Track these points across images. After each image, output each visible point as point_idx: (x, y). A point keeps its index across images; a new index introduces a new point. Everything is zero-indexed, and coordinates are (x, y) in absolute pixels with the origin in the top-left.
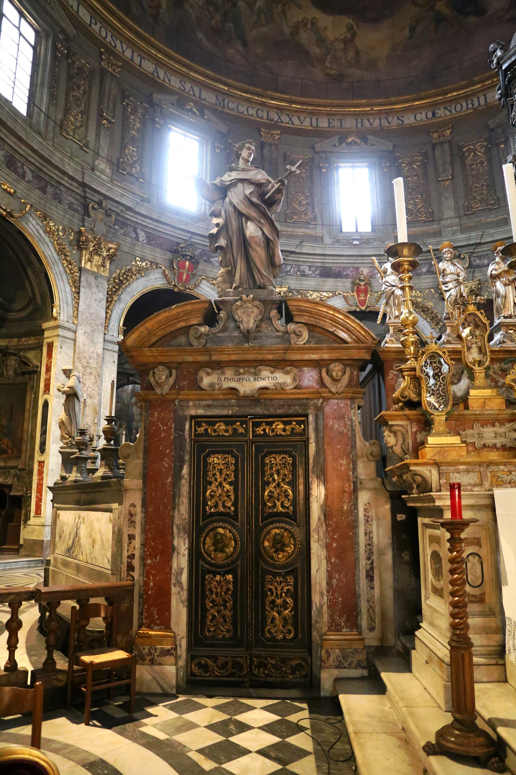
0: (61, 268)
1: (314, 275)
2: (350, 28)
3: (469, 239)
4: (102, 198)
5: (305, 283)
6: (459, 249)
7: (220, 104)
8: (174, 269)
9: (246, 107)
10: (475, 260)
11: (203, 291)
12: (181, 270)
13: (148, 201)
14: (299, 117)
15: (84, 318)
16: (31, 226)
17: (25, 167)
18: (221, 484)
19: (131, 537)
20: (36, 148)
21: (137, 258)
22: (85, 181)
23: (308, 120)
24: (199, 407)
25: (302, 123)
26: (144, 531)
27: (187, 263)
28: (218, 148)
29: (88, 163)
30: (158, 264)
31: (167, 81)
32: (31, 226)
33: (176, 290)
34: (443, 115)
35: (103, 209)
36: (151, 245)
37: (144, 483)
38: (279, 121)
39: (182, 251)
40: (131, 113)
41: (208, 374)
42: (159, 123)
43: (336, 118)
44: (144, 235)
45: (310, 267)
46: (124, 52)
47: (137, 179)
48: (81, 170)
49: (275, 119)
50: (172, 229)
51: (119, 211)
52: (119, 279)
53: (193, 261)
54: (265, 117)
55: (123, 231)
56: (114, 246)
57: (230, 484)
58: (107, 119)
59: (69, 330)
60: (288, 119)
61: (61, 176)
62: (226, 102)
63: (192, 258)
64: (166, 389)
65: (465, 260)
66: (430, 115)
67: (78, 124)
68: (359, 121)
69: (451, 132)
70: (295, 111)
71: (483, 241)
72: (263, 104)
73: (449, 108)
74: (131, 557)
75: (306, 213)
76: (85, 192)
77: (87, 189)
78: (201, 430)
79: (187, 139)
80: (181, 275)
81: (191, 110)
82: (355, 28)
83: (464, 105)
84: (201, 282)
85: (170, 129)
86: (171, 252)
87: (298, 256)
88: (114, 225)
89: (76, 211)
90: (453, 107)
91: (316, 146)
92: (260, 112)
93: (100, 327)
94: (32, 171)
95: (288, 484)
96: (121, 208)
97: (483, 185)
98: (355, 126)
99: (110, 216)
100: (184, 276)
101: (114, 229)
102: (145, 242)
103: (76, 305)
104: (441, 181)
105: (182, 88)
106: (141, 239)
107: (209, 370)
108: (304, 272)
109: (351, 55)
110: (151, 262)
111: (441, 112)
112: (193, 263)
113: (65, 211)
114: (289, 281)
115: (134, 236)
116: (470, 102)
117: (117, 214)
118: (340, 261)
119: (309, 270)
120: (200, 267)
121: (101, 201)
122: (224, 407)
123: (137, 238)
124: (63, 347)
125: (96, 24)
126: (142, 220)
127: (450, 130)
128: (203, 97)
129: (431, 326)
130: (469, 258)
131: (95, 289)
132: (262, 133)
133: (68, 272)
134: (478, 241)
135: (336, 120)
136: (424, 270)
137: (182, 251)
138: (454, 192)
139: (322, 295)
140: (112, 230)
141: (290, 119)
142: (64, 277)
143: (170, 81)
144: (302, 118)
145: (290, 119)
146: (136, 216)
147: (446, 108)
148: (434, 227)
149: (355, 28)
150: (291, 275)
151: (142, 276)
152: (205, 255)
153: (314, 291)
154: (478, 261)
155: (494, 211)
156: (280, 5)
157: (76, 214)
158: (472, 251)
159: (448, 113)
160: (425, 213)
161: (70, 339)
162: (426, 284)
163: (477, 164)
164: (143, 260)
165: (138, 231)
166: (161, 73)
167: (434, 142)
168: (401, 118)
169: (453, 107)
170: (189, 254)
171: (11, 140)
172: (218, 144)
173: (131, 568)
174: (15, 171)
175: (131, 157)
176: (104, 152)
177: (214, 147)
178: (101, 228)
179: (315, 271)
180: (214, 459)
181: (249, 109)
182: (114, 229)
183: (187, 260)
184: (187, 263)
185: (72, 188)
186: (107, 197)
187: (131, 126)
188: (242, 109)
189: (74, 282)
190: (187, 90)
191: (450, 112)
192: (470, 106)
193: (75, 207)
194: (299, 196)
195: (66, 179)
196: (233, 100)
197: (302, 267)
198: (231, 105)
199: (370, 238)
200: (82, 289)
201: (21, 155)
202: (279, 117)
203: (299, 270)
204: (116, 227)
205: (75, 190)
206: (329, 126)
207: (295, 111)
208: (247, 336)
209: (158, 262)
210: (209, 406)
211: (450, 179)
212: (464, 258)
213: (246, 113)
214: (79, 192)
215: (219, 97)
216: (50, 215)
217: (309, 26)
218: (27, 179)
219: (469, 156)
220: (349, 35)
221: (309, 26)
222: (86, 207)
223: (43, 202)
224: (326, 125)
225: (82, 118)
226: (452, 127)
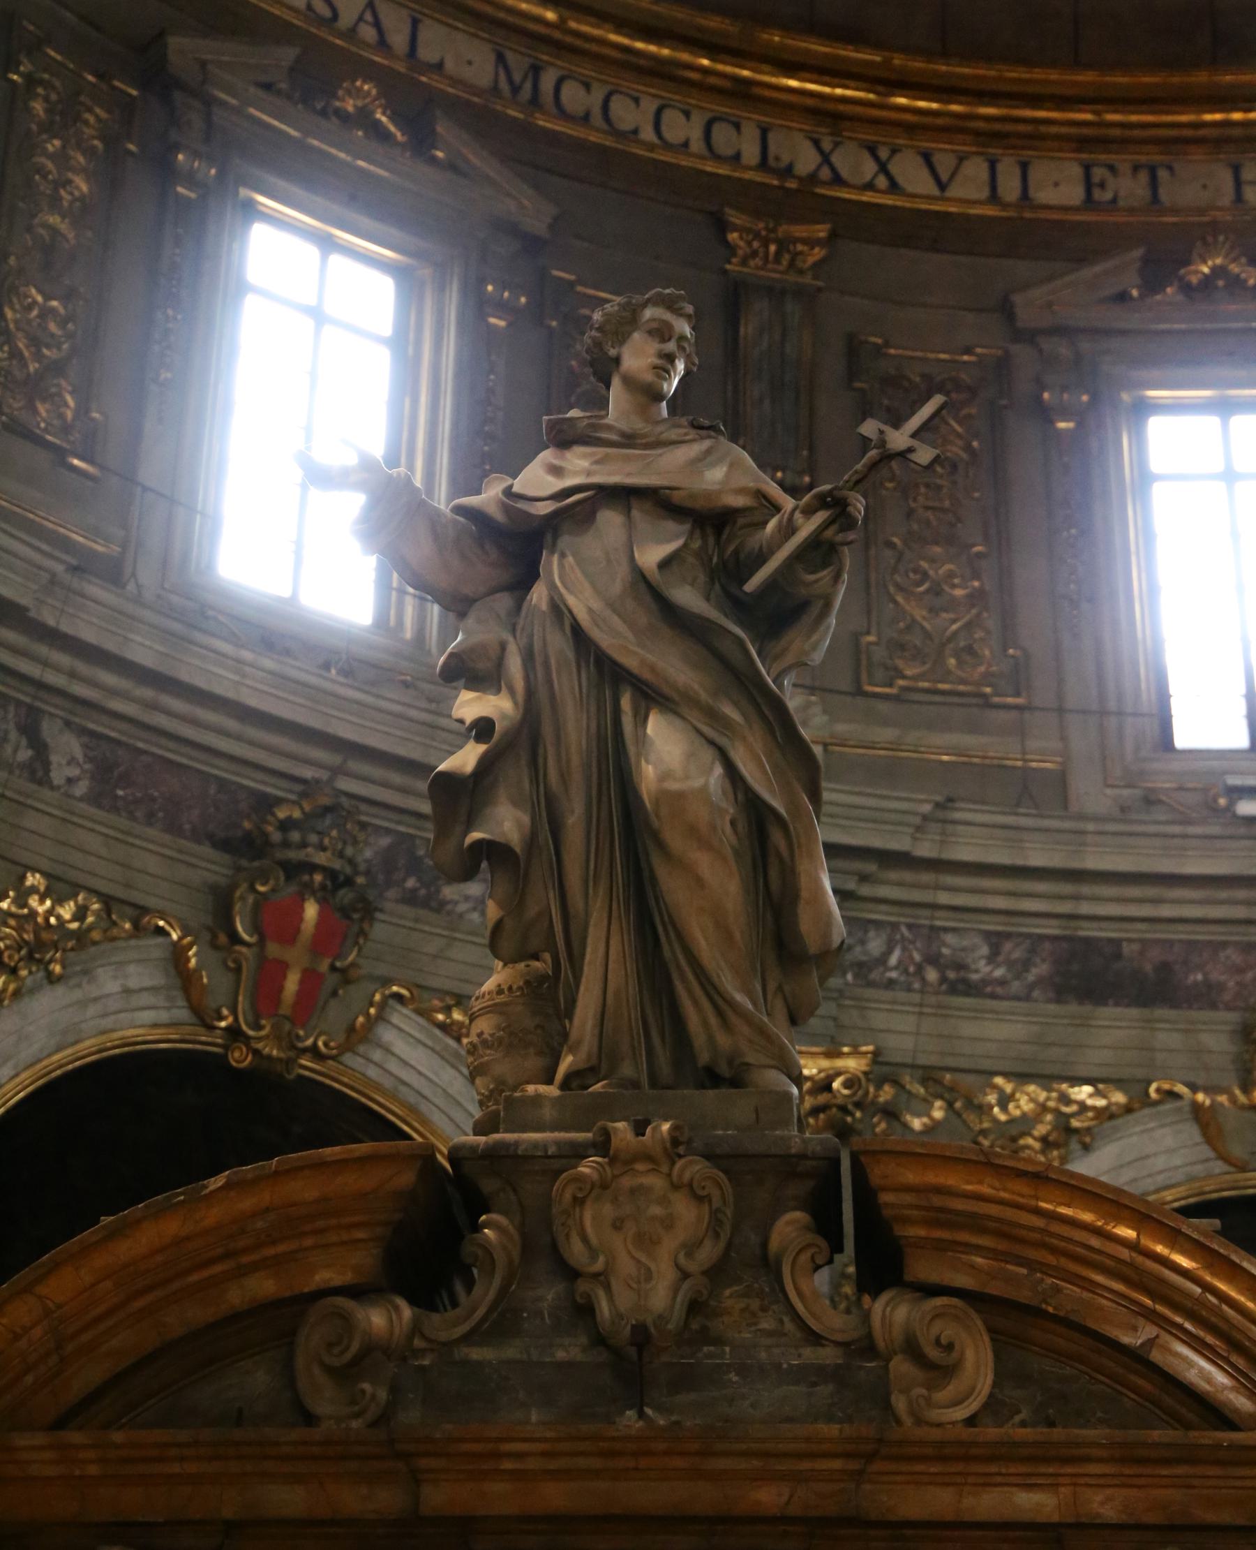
1: (1016, 986)
5: (969, 1029)
7: (516, 90)
8: (235, 938)
9: (649, 106)
11: (393, 1066)
12: (273, 949)
14: (927, 157)
21: (32, 880)
23: (976, 169)
25: (942, 186)
27: (311, 911)
28: (502, 308)
30: (144, 910)
33: (239, 1058)
36: (115, 809)
38: (825, 173)
39: (286, 844)
40: (49, 129)
42: (191, 180)
43: (1123, 161)
44: (78, 753)
45: (996, 940)
47: (60, 454)
50: (232, 724)
53: (345, 896)
54: (751, 153)
60: (869, 168)
62: (548, 81)
63: (337, 881)
70: (910, 129)
72: (742, 92)
75: (970, 650)
79: (336, 259)
80: (271, 973)
81: (363, 119)
84: (380, 1017)
85: (250, 212)
86: (224, 845)
87: (927, 877)
91: (1017, 299)
92: (722, 134)
100: (292, 984)
102: (81, 789)
106: (57, 777)
108: (960, 966)
110: (109, 902)
112: (345, 912)
114: (879, 1020)
115: (25, 754)
118: (1166, 911)
119: (992, 959)
120: (379, 931)
123: (38, 769)
126: (72, 675)
128: (427, 53)
132: (733, 237)
135: (1125, 168)
137: (286, 844)
139: (1065, 1099)
144: (944, 163)
145: (883, 168)
146: (43, 650)
150: (891, 984)
151: (52, 979)
152: (414, 866)
153: (1022, 1078)
164: (59, 889)
165: (49, 730)
170: (321, 858)
175: (35, 342)
179: (1026, 964)
181: (668, 115)
183: (307, 890)
184: (311, 911)
187: (45, 188)
188: (626, 114)
190: (345, 21)
194: (932, 561)
196: (587, 71)
197: (950, 938)
198: (573, 96)
202: (826, 159)
203: (933, 959)
207: (910, 129)
209: (151, 902)
213: (648, 134)
215: (510, 57)
224: (1072, 193)
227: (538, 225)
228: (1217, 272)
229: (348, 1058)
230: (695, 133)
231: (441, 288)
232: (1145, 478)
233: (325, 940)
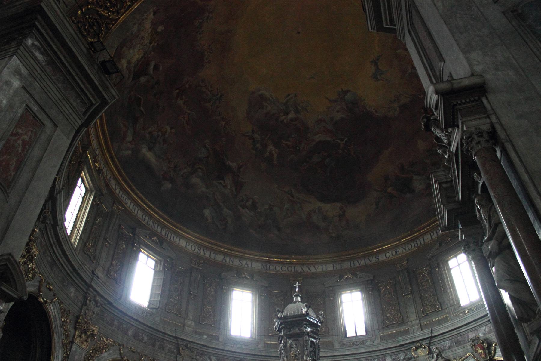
2: (341, 208)
3: (424, 334)
4: (188, 343)
6: (420, 342)
7: (264, 268)
9: (281, 266)
13: (217, 338)
17: (143, 335)
22: (177, 336)
25: (316, 270)
28: (263, 296)
29: (181, 323)
31: (231, 262)
34: (402, 253)
38: (302, 271)
46: (205, 254)
47: (211, 325)
49: (299, 271)
51: (198, 348)
55: (202, 359)
58: (193, 295)
60: (307, 269)
62: (268, 267)
65: (426, 349)
66: (394, 253)
67: (176, 302)
68: (352, 262)
69: (407, 263)
71: (434, 335)
73: (404, 248)
76: (178, 341)
77: (178, 340)
81: (245, 277)
82: (344, 208)
83: (413, 245)
85: (233, 290)
90: (407, 246)
94: (147, 336)
96: (199, 346)
98: (349, 267)
101: (196, 359)
104: (405, 295)
105: (240, 264)
109: (344, 223)
111: (400, 251)
113: (166, 354)
116: (415, 243)
117: (198, 349)
118: (345, 359)
121: (187, 344)
125: (189, 245)
127: (406, 262)
130: (429, 347)
134: (430, 335)
135: (338, 264)
141: (309, 269)
143: (233, 262)
145: (309, 269)
147: (403, 248)
149: (344, 208)
155: (439, 313)
156: (298, 205)
158: (429, 342)
159: (404, 251)
163: (425, 282)
165: (212, 357)
166: (228, 259)
167: (398, 270)
168: (378, 257)
169: (407, 246)
172: (262, 293)
175: (208, 312)
176: (191, 316)
177: (260, 296)
185: (170, 340)
186: (190, 342)
191: (405, 250)
192: (416, 245)
193: (172, 350)
195: (167, 336)
199: (364, 339)
202: (302, 269)
205: (172, 341)
206: (334, 269)
211: (410, 294)
212: (425, 348)
213: (280, 270)
217: (317, 212)
219: (420, 276)
220: (341, 212)
221: (317, 212)
222: (178, 348)
225: (179, 297)
226: (407, 260)
227: (267, 285)
228: (348, 276)
230: (286, 269)
231: (256, 295)
232: (342, 303)
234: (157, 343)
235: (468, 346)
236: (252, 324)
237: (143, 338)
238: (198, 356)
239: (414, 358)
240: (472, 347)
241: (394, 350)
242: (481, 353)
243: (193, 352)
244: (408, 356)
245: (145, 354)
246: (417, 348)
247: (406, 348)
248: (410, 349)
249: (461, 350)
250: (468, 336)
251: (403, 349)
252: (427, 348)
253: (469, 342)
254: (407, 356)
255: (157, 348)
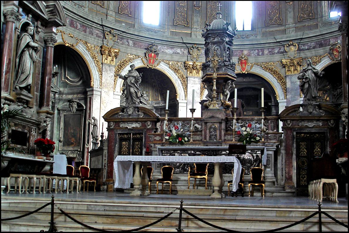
0: (94, 64)
6: (293, 41)
8: (147, 58)
10: (301, 47)
11: (161, 67)
15: (105, 85)
16: (81, 48)
17: (77, 23)
18: (125, 148)
19: (105, 160)
20: (81, 15)
24: (120, 131)
26: (108, 158)
27: (153, 54)
32: (81, 48)
35: (112, 34)
37: (108, 148)
41: (122, 124)
48: (101, 20)
52: (120, 65)
56: (117, 51)
57: (127, 148)
59: (98, 91)
61: (93, 23)
63: (155, 52)
64: (113, 127)
74: (105, 164)
76: (103, 28)
77: (104, 27)
78: (121, 136)
86: (146, 49)
88: (117, 40)
89: (100, 37)
93: (112, 89)
95: (139, 148)
97: (308, 5)
99: (115, 36)
100: (152, 61)
103: (101, 80)
106: (130, 45)
107: (122, 123)
110: (135, 55)
113: (95, 39)
115: (127, 43)
117: (119, 35)
121: (111, 31)
122: (126, 131)
123: (128, 45)
124: (96, 99)
129: (277, 81)
130: (298, 45)
131: (109, 72)
133: (97, 66)
134: (301, 37)
136: (276, 51)
138: (294, 9)
140: (116, 43)
142: (95, 68)
148: (283, 28)
152: (163, 48)
154: (303, 47)
157: (100, 39)
160: (278, 20)
161: (98, 95)
162: (276, 59)
165: (129, 41)
170: (153, 50)
171: (71, 15)
173: (105, 166)
174: (73, 27)
178: (111, 43)
180: (124, 143)
182: (117, 42)
184: (153, 54)
185: (97, 27)
189: (99, 69)
193: (99, 35)
195: (94, 24)
200: (103, 73)
201: (75, 19)
204: (118, 41)
208: (130, 115)
209: (139, 55)
210: (122, 131)
214: (100, 28)
216: (88, 41)
218: (78, 28)
223: (85, 36)
229: (157, 66)
233: (155, 57)
234: (88, 30)
235: (328, 48)
236: (161, 15)
237: (77, 25)
238: (119, 40)
239: (286, 52)
240: (330, 50)
241: (272, 45)
242: (336, 55)
243: (115, 36)
244: (282, 50)
245: (80, 38)
246: (289, 45)
247: (281, 45)
248: (284, 46)
249: (322, 51)
250: (330, 41)
251: (279, 45)
252: (297, 45)
253: (329, 45)
254: (280, 51)
255: (88, 33)
